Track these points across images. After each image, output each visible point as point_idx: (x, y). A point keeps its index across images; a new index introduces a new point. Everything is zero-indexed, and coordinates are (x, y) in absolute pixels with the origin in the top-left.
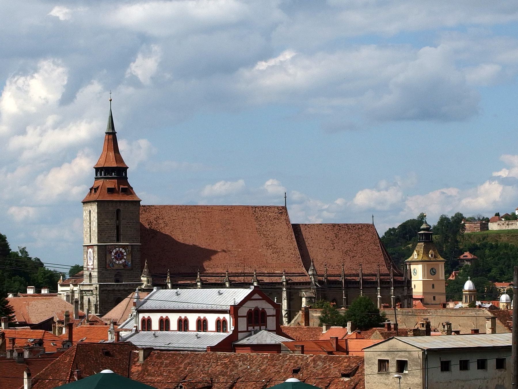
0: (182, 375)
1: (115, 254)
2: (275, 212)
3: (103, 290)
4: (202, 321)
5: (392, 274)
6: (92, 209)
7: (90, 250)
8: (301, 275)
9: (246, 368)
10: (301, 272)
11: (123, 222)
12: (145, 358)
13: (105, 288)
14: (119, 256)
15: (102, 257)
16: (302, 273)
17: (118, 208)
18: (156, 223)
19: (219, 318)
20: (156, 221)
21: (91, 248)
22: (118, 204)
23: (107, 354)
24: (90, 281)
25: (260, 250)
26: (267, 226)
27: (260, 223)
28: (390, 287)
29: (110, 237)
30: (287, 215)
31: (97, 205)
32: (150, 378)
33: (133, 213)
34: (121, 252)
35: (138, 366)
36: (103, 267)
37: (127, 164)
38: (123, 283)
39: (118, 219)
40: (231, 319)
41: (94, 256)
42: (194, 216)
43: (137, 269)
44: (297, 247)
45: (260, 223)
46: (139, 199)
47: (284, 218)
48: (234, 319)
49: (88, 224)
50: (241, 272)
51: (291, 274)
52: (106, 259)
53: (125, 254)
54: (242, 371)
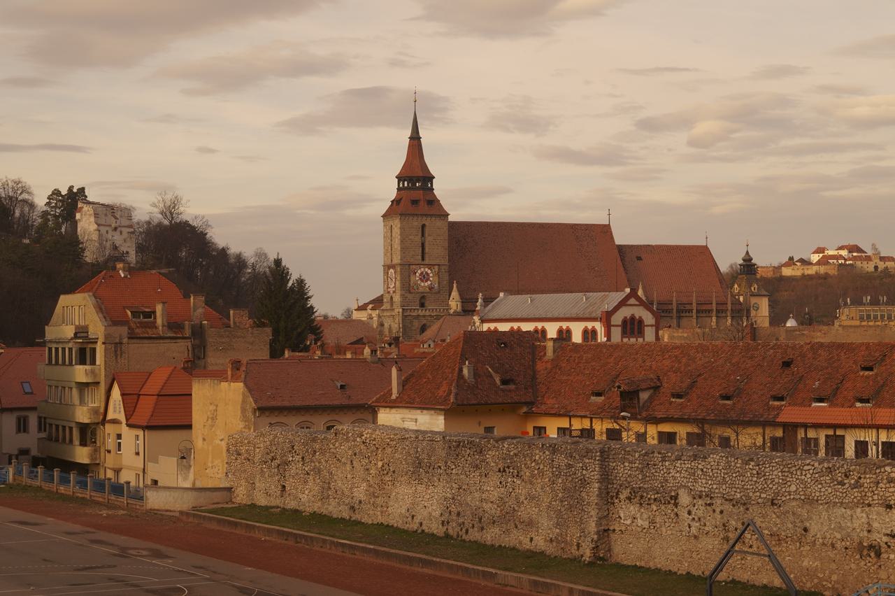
0: (614, 372)
1: (420, 275)
3: (406, 316)
4: (564, 332)
5: (729, 303)
11: (428, 239)
13: (408, 313)
14: (424, 277)
19: (586, 327)
24: (392, 305)
28: (727, 317)
32: (565, 378)
34: (426, 273)
37: (433, 172)
40: (603, 328)
49: (389, 241)
52: (410, 281)
53: (431, 275)
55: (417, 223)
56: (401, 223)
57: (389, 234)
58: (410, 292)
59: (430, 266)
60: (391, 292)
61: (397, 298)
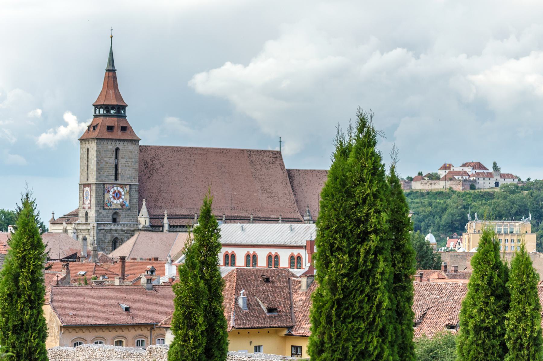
2: (269, 156)
3: (100, 230)
4: (273, 257)
6: (90, 147)
7: (87, 189)
8: (296, 220)
9: (436, 298)
10: (296, 217)
11: (122, 161)
12: (308, 286)
13: (102, 227)
14: (117, 195)
15: (100, 196)
16: (297, 219)
17: (117, 146)
18: (152, 163)
19: (292, 253)
20: (152, 162)
21: (88, 186)
22: (118, 142)
23: (267, 280)
24: (87, 219)
25: (255, 194)
26: (262, 170)
27: (255, 167)
29: (108, 175)
30: (282, 159)
31: (96, 143)
33: (132, 152)
35: (301, 294)
36: (101, 207)
38: (121, 223)
39: (116, 157)
40: (307, 255)
41: (92, 194)
42: (190, 158)
43: (134, 209)
44: (291, 192)
45: (255, 167)
46: (138, 138)
47: (279, 163)
48: (310, 255)
49: (86, 162)
50: (237, 216)
51: (287, 219)
52: (104, 198)
53: (123, 193)
54: (431, 301)
55: (111, 146)
56: (97, 147)
57: (85, 156)
58: (104, 209)
59: (122, 186)
60: (87, 208)
61: (92, 214)
